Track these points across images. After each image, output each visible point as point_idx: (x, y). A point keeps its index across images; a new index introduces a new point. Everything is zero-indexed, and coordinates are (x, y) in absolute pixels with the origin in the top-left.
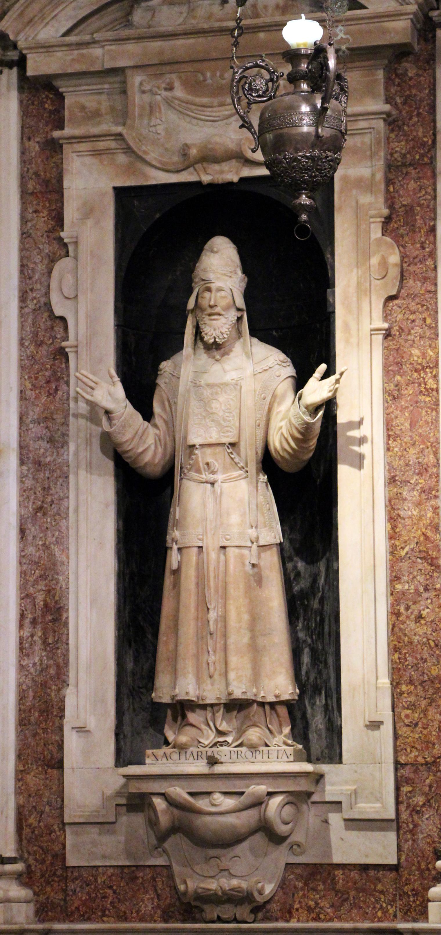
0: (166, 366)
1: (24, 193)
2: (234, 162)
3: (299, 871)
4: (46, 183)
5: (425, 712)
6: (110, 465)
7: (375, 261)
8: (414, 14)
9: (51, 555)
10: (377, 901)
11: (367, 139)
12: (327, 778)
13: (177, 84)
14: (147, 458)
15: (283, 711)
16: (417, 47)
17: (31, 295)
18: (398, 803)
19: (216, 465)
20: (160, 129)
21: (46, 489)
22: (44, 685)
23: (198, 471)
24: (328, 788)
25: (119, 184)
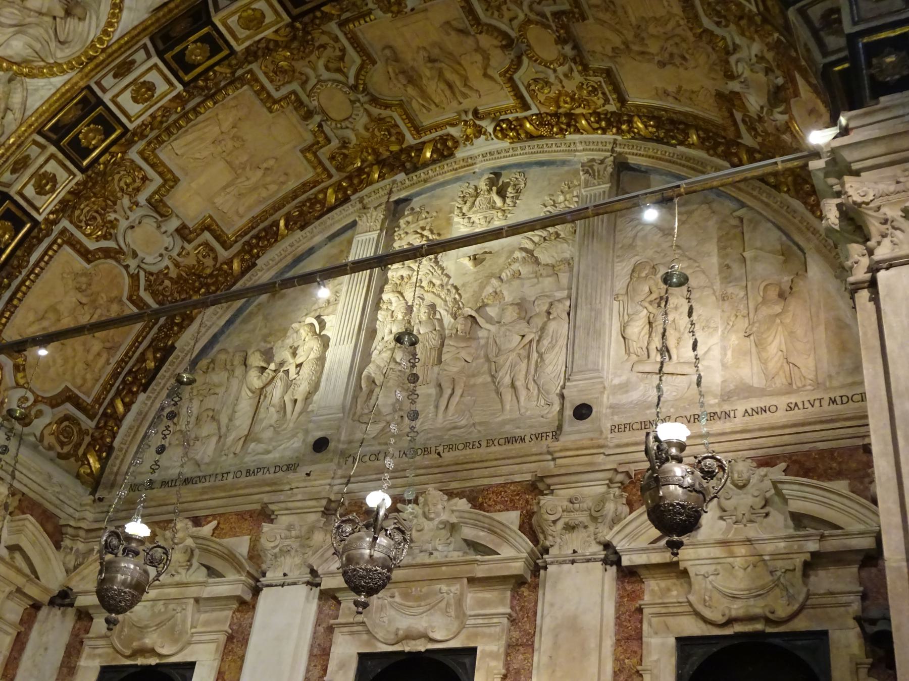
1: (311, 655)
2: (423, 639)
4: (324, 649)
8: (526, 558)
11: (498, 629)
13: (397, 594)
16: (529, 580)
20: (385, 619)
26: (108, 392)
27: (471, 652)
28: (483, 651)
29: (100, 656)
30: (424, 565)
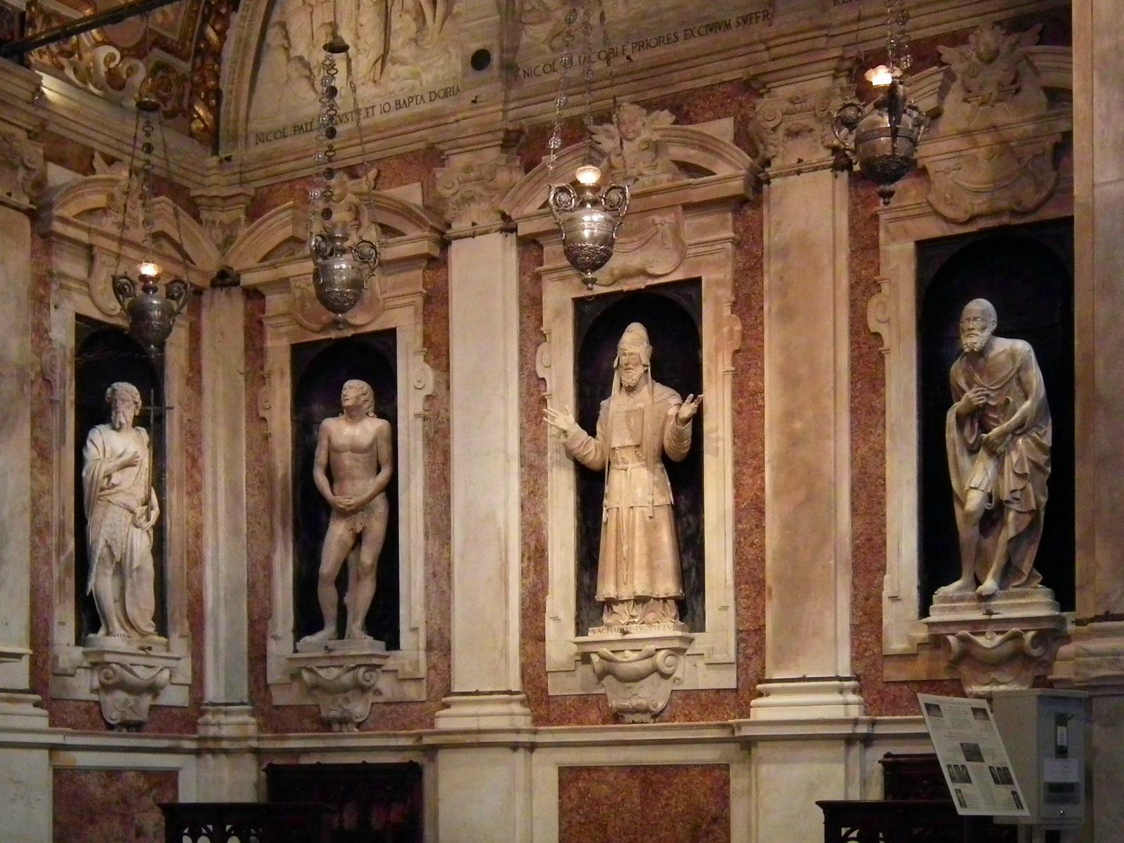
0: (604, 403)
1: (522, 307)
5: (755, 600)
6: (571, 464)
9: (539, 518)
12: (696, 640)
14: (591, 458)
15: (671, 602)
17: (525, 367)
18: (738, 652)
19: (628, 458)
21: (536, 481)
23: (618, 463)
24: (697, 646)
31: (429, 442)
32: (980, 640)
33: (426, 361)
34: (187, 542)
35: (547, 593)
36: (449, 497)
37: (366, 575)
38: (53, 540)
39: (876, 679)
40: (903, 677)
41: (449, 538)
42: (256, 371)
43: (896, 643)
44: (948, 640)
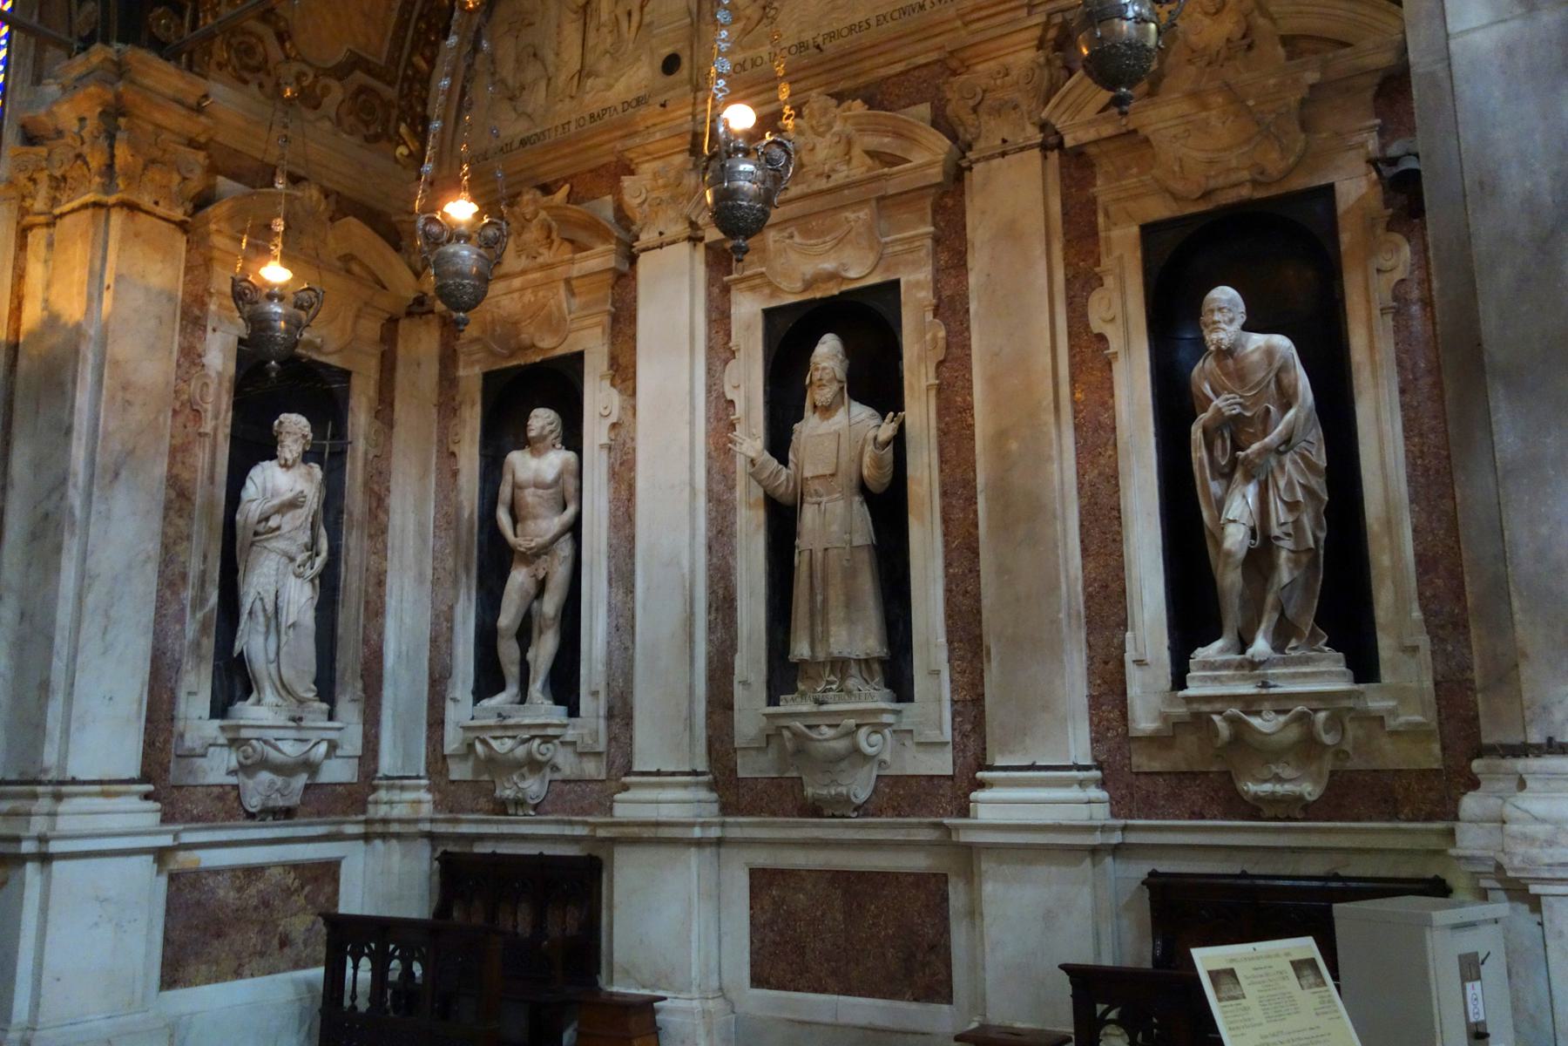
0: (796, 425)
1: (710, 322)
3: (886, 780)
4: (723, 313)
7: (928, 337)
9: (727, 563)
10: (940, 802)
13: (796, 233)
15: (876, 667)
21: (724, 518)
22: (723, 652)
25: (765, 306)
26: (402, 48)
27: (895, 284)
28: (908, 283)
29: (478, 361)
30: (821, 193)
31: (614, 475)
32: (1256, 721)
33: (613, 385)
34: (366, 591)
35: (735, 651)
36: (633, 538)
37: (548, 627)
38: (188, 594)
39: (1122, 768)
40: (1156, 766)
41: (633, 586)
42: (448, 407)
43: (1144, 721)
44: (1212, 720)
